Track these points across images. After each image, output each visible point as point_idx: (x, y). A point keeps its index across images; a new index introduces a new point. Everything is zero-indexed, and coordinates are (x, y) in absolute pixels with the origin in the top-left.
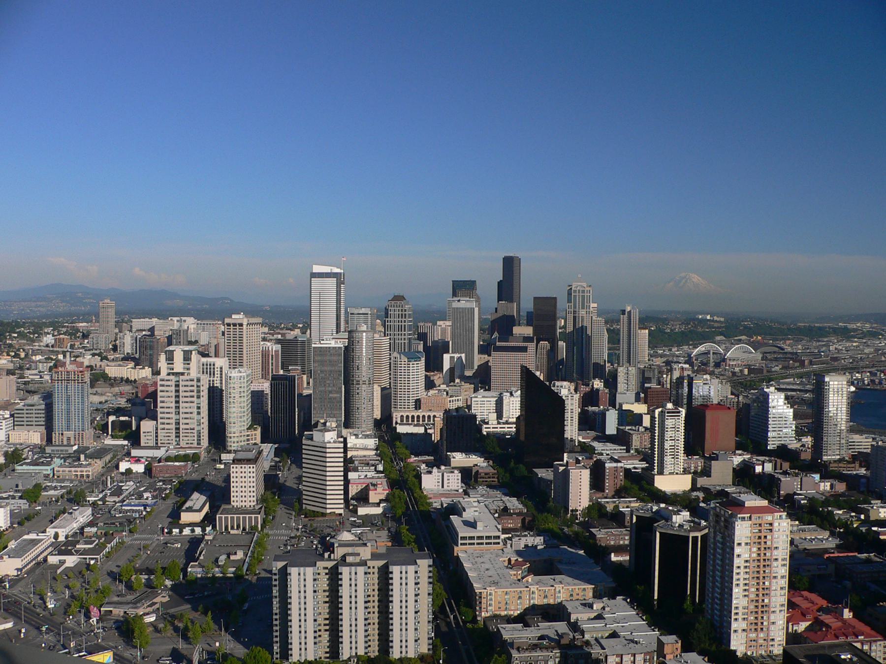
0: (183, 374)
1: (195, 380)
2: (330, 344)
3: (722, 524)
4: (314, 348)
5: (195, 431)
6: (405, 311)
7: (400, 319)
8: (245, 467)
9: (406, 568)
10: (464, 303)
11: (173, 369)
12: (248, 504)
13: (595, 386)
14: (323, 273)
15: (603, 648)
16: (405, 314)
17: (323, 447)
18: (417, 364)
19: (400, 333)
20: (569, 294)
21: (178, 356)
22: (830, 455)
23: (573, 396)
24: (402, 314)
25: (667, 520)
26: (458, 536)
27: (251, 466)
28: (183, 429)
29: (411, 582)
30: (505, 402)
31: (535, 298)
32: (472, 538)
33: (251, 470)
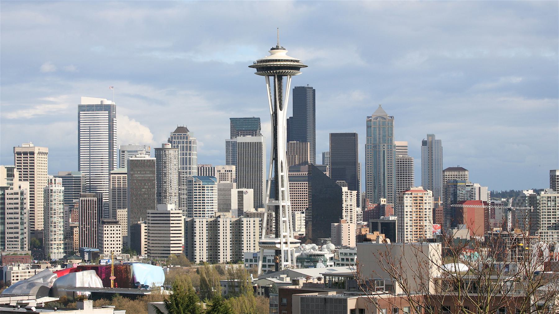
0: (7, 188)
1: (19, 194)
2: (145, 157)
5: (19, 240)
6: (190, 142)
7: (185, 152)
9: (250, 219)
13: (382, 203)
14: (93, 106)
16: (190, 147)
17: (167, 214)
18: (211, 187)
19: (185, 166)
20: (369, 127)
23: (352, 192)
24: (187, 147)
27: (118, 226)
28: (8, 238)
29: (252, 225)
33: (118, 229)
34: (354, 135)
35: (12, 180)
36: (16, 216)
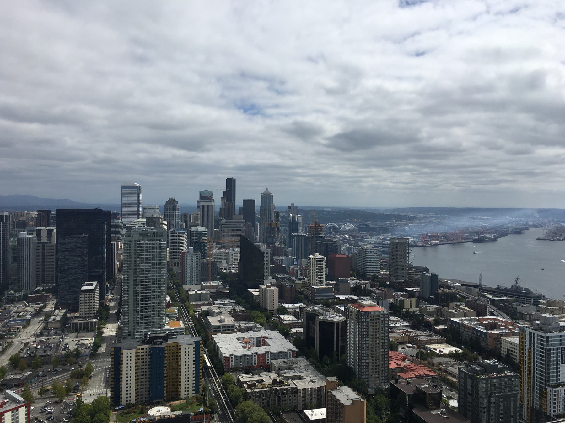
0: (47, 243)
3: (354, 317)
4: (127, 227)
7: (173, 211)
8: (88, 294)
10: (206, 203)
11: (41, 240)
12: (89, 315)
14: (128, 186)
15: (296, 385)
16: (176, 209)
21: (44, 234)
22: (399, 280)
25: (322, 315)
26: (212, 327)
27: (92, 294)
30: (230, 254)
31: (244, 200)
32: (219, 327)
33: (92, 296)
34: (253, 201)
35: (51, 237)
36: (52, 260)
